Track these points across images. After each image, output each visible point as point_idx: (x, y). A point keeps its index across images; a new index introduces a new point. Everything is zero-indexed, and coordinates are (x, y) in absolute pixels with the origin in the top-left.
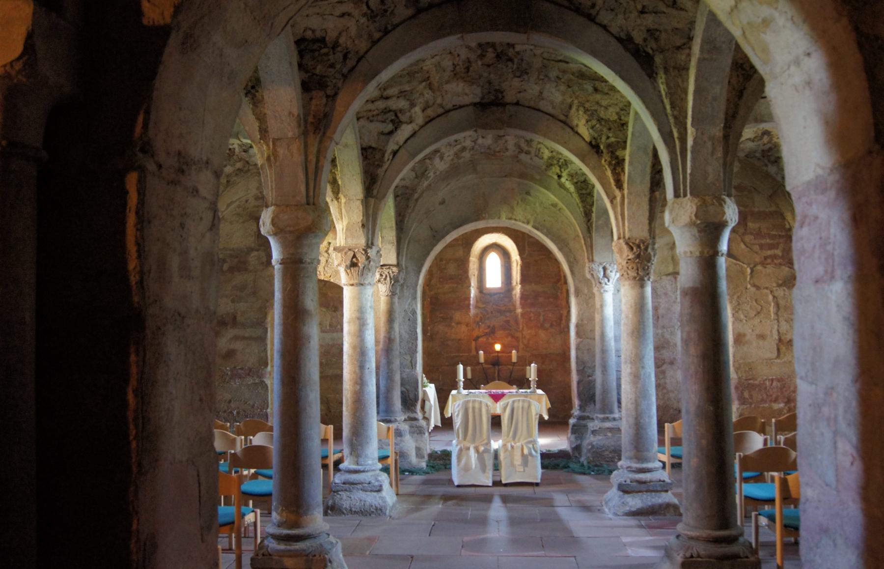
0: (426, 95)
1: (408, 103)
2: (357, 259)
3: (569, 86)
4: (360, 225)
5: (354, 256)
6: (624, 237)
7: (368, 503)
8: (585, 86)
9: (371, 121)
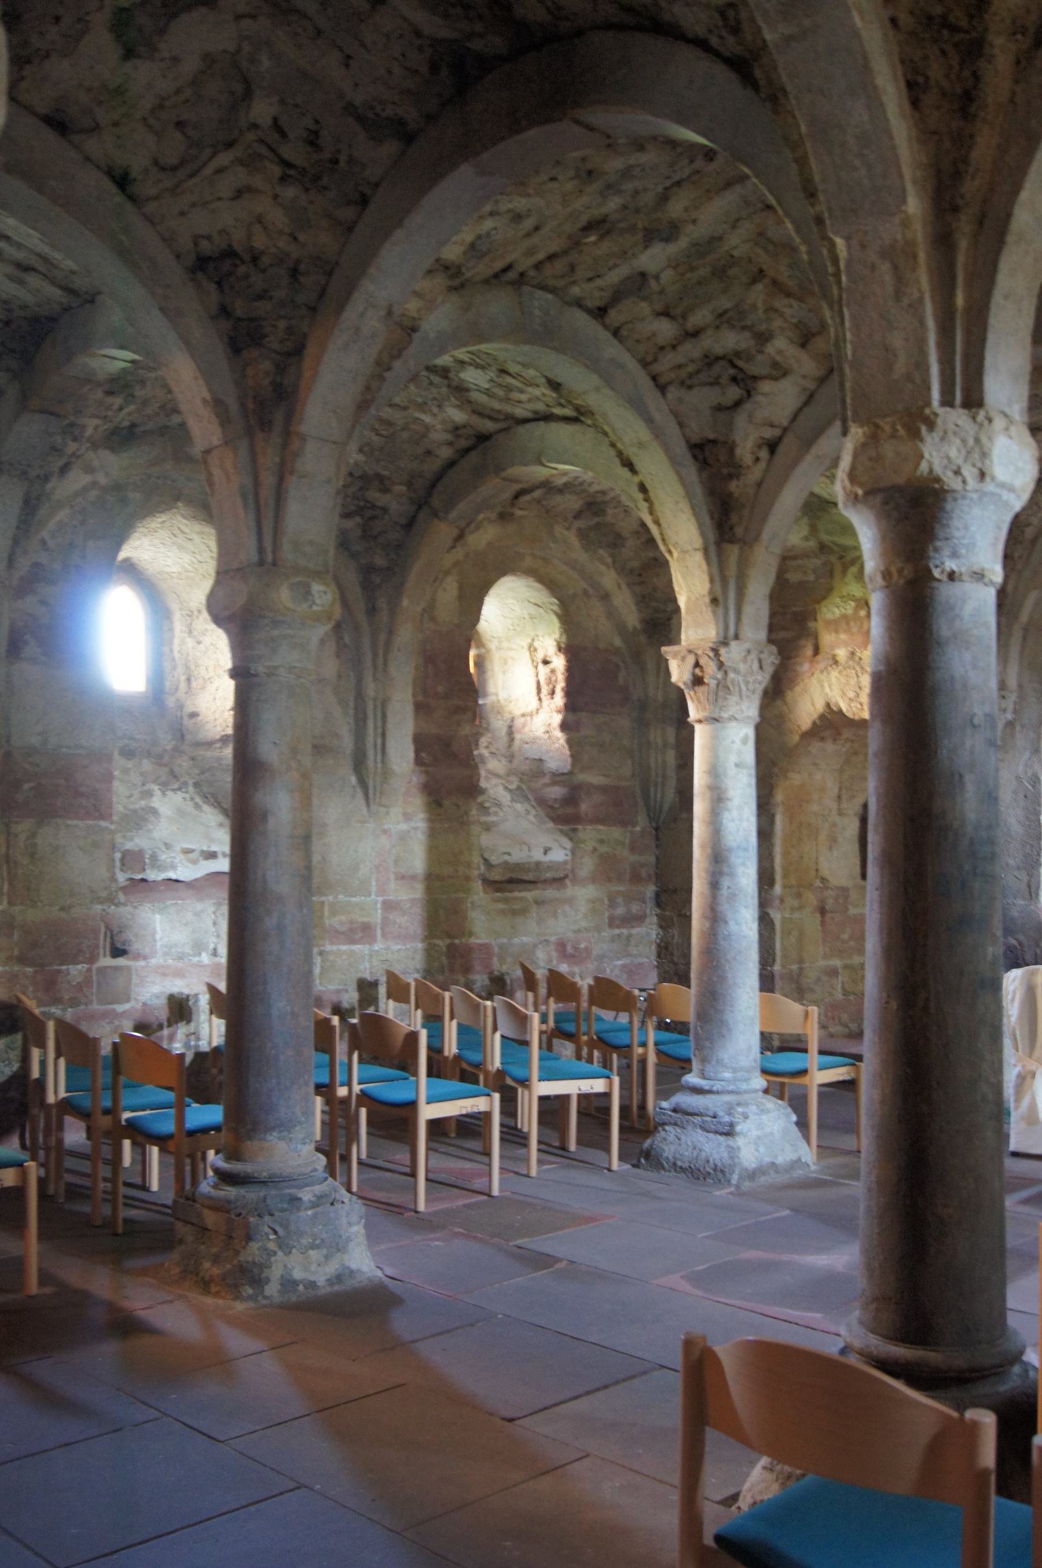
0: (788, 311)
1: (747, 334)
2: (701, 668)
4: (707, 600)
5: (697, 665)
7: (704, 1154)
9: (690, 387)
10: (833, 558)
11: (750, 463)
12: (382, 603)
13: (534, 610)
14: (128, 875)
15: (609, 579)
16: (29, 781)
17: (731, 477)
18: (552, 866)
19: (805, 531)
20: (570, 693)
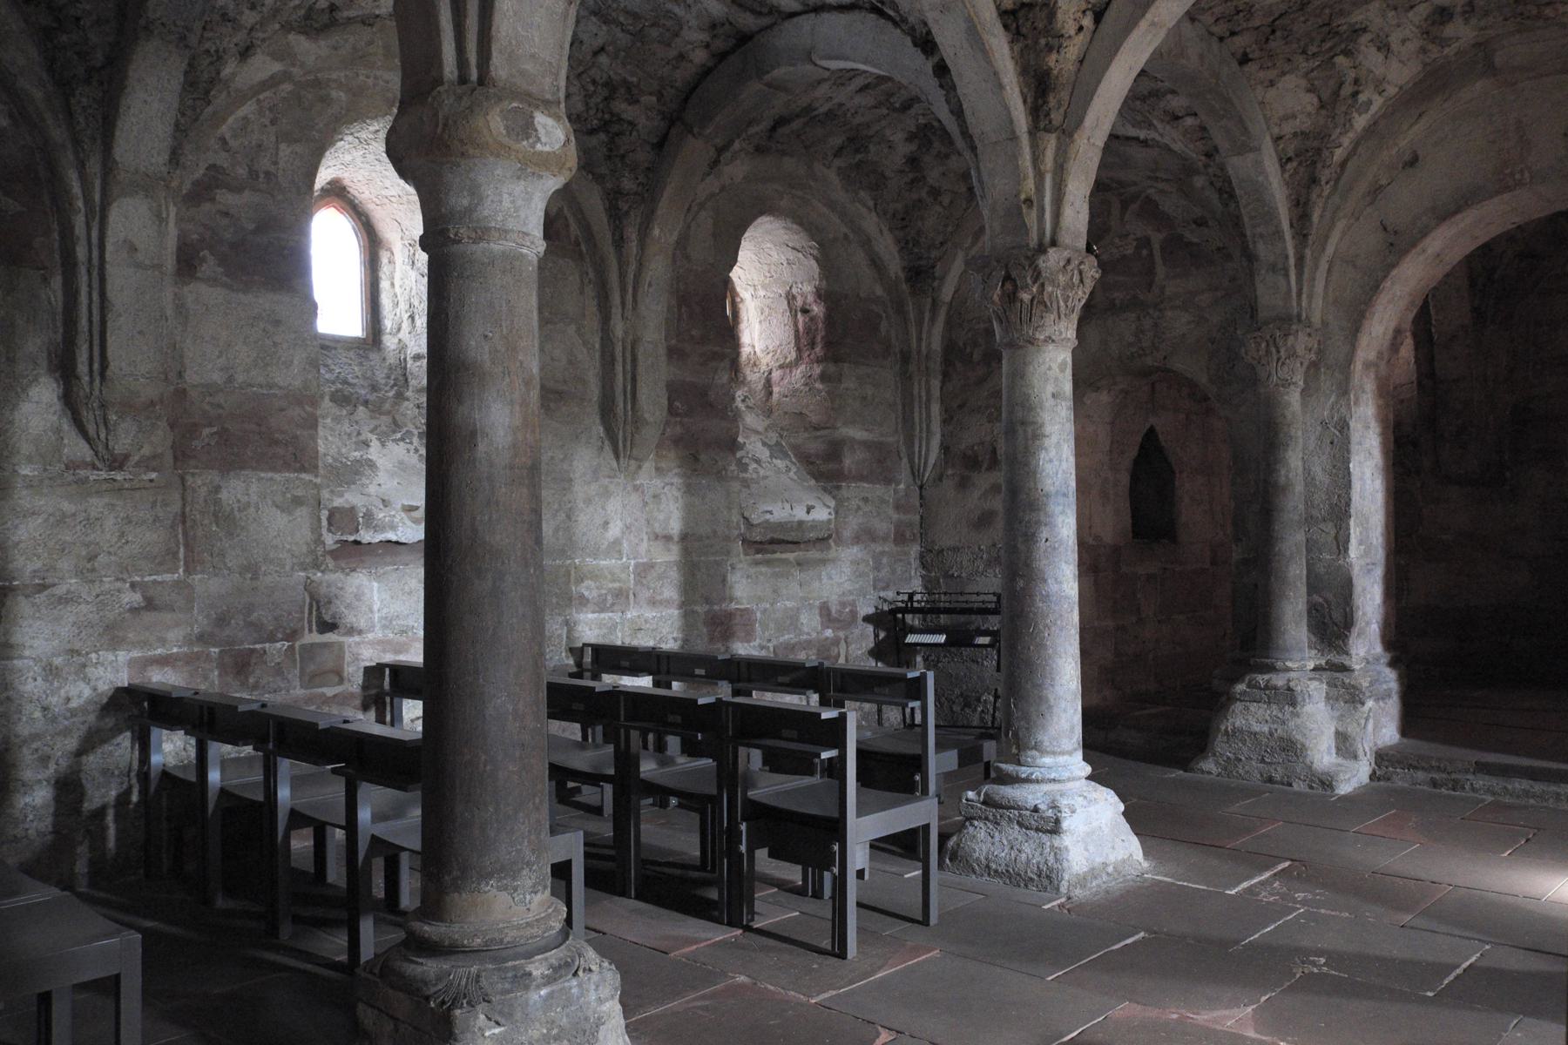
11: (1072, 32)
12: (632, 233)
13: (792, 255)
14: (338, 537)
15: (871, 223)
16: (210, 425)
17: (1050, 48)
18: (815, 525)
20: (828, 344)
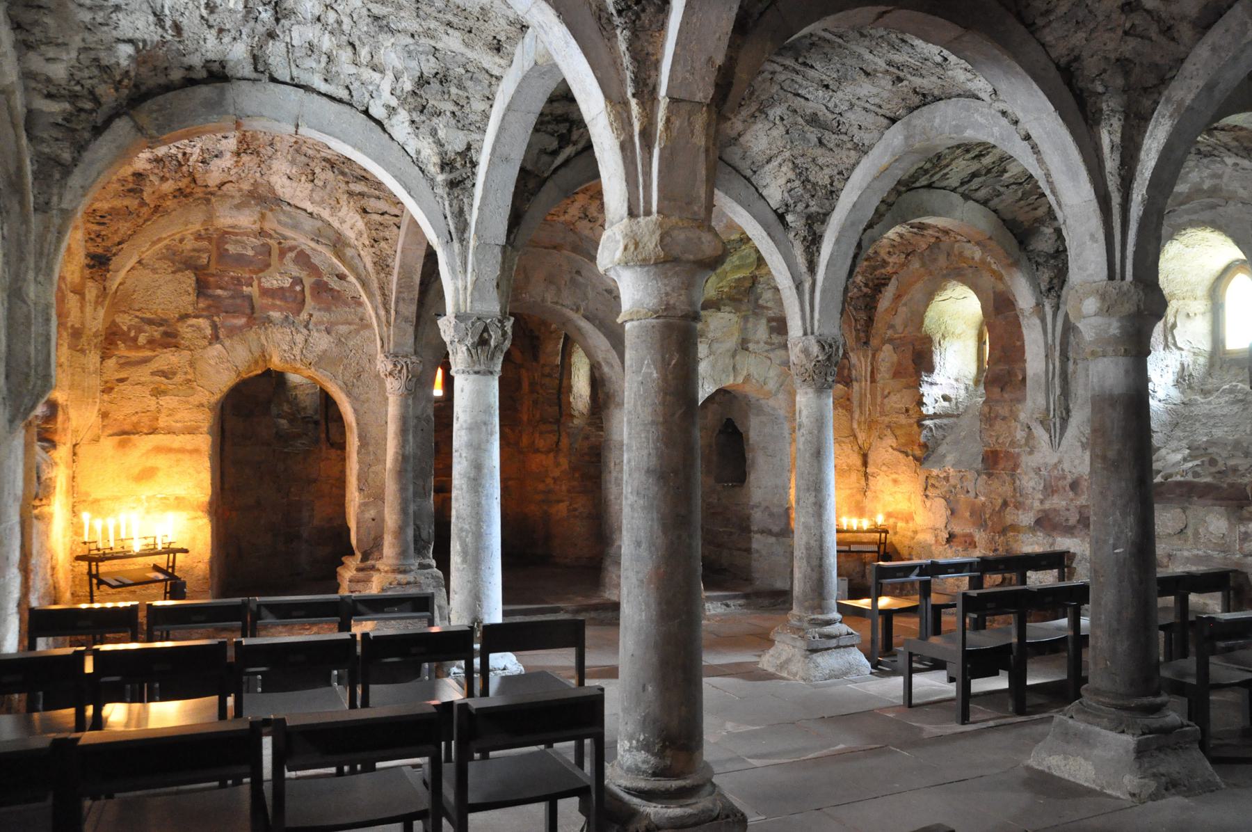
2: (490, 336)
3: (787, 132)
5: (486, 329)
6: (812, 333)
8: (808, 135)
10: (271, 242)
19: (256, 217)
